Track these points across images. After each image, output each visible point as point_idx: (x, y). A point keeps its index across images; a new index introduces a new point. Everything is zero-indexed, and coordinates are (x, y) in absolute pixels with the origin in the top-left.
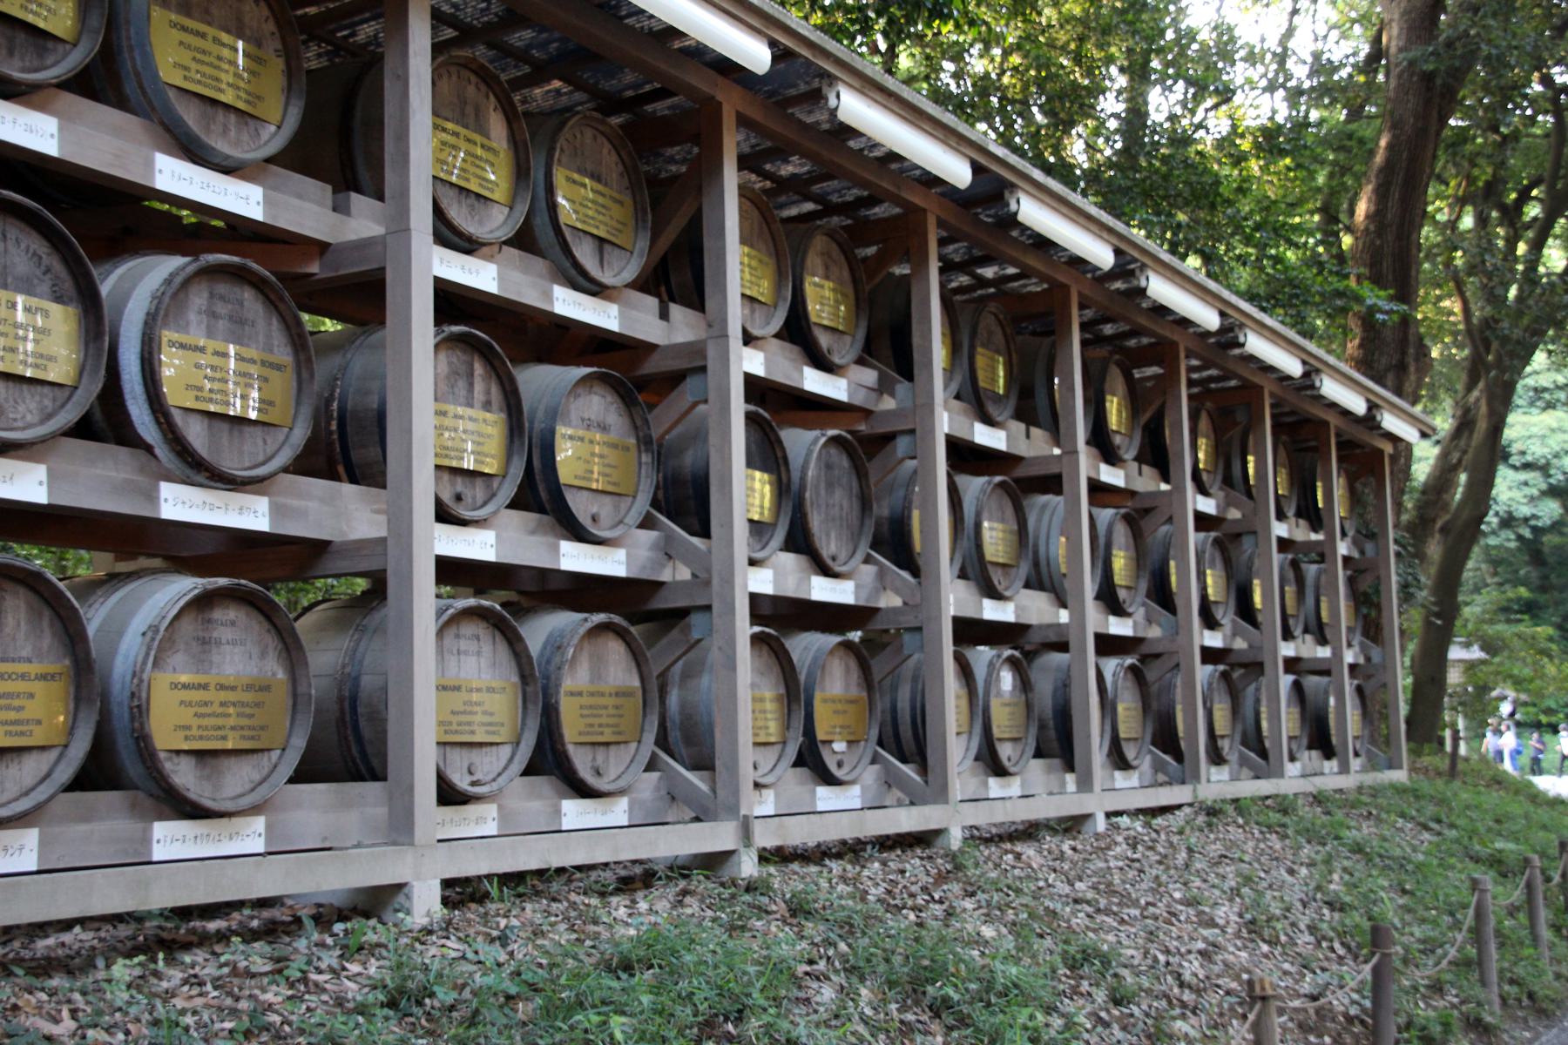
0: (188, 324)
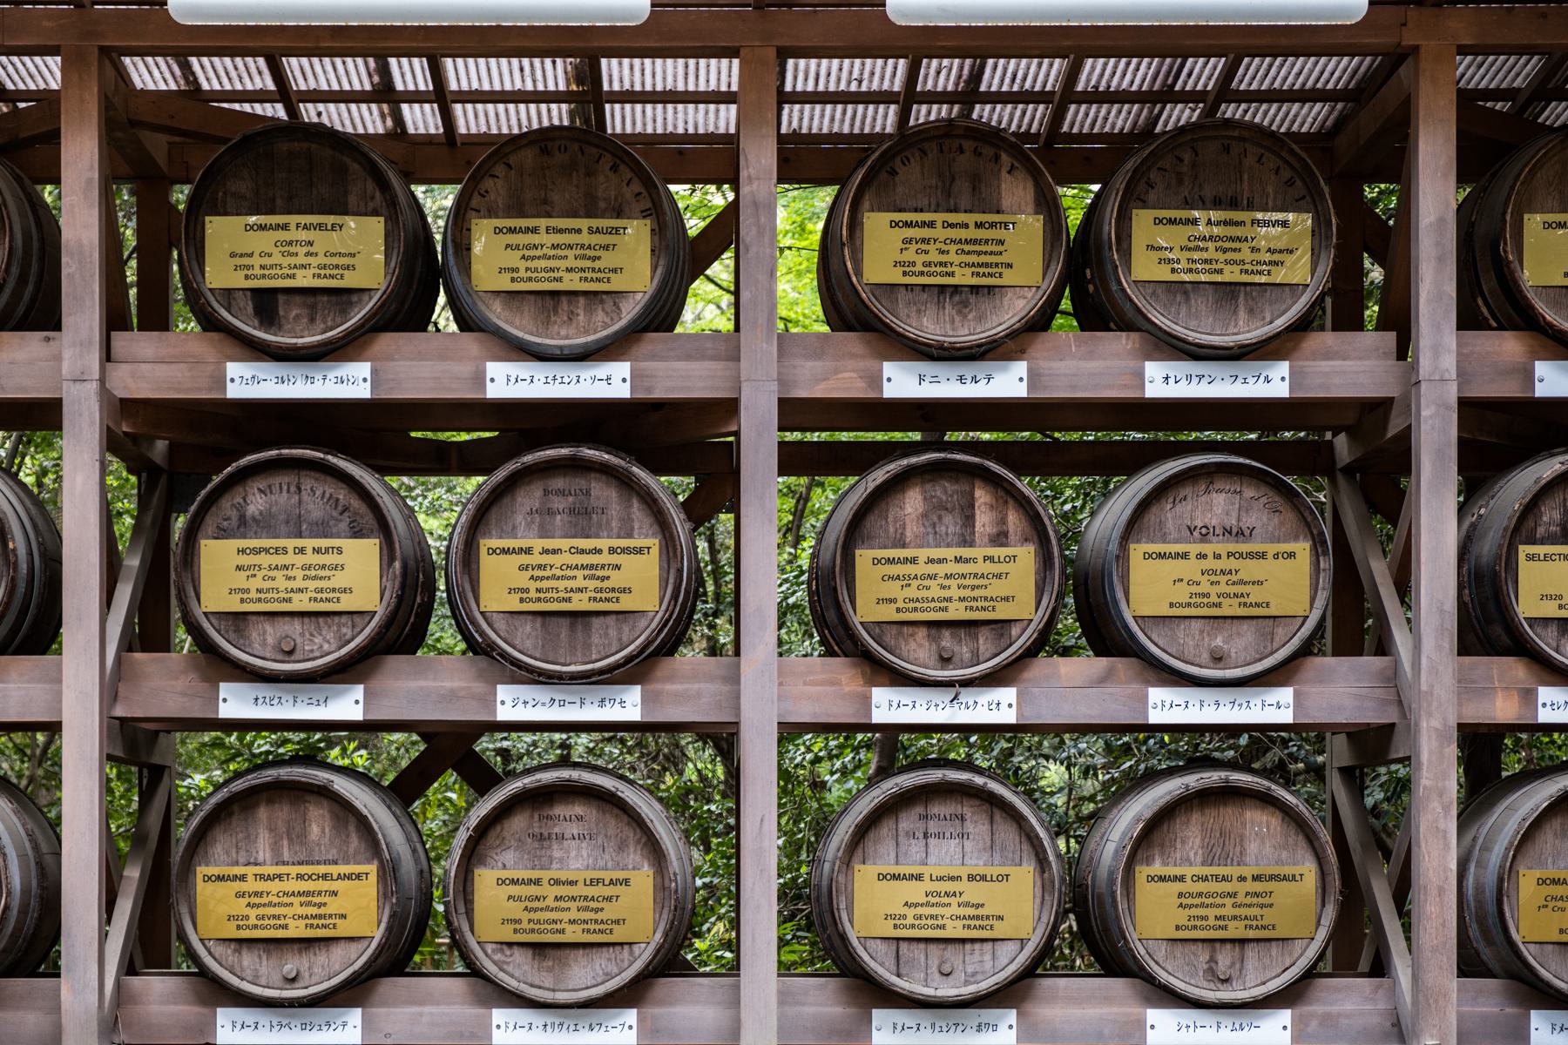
0: (514, 527)
